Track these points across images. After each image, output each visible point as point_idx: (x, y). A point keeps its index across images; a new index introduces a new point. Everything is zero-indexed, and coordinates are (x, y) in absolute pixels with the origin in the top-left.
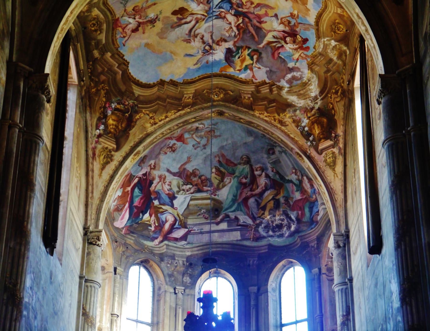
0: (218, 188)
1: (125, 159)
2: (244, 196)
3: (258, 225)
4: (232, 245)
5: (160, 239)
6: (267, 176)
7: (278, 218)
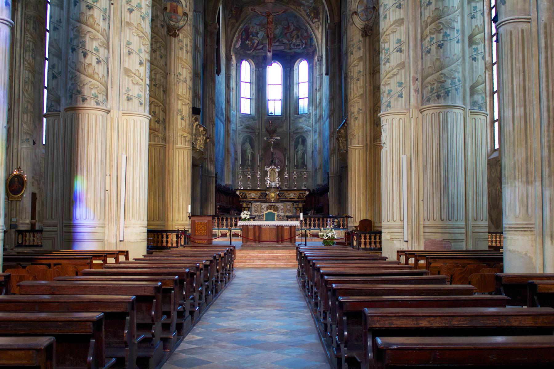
0: (275, 29)
1: (239, 25)
2: (285, 32)
3: (291, 44)
4: (281, 51)
5: (253, 50)
6: (294, 26)
7: (298, 42)
